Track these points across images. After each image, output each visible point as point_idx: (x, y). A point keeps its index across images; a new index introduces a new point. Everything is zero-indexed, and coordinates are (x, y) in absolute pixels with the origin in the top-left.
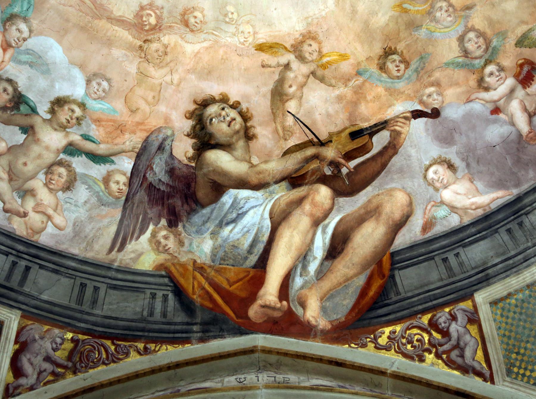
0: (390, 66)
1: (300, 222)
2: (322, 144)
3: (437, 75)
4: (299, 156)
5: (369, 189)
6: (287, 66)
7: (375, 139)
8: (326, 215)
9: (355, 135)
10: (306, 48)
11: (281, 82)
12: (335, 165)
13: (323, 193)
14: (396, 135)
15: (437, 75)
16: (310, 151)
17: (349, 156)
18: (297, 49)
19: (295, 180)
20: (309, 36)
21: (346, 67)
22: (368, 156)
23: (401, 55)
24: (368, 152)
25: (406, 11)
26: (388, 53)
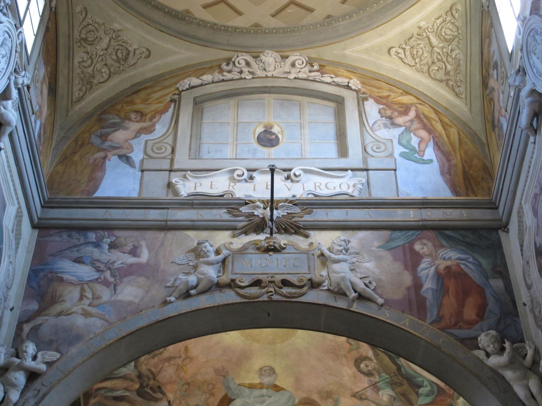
0: (184, 387)
1: (125, 384)
2: (154, 379)
3: (183, 402)
4: (149, 373)
5: (141, 399)
6: (181, 357)
7: (159, 394)
8: (128, 391)
9: (159, 387)
10: (187, 360)
11: (175, 358)
12: (147, 386)
13: (137, 386)
14: (161, 399)
15: (183, 402)
16: (151, 376)
17: (152, 389)
18: (187, 357)
19: (140, 376)
20: (191, 359)
21: (182, 374)
22: (152, 394)
23: (189, 388)
24: (154, 393)
25: (203, 384)
26: (188, 384)
